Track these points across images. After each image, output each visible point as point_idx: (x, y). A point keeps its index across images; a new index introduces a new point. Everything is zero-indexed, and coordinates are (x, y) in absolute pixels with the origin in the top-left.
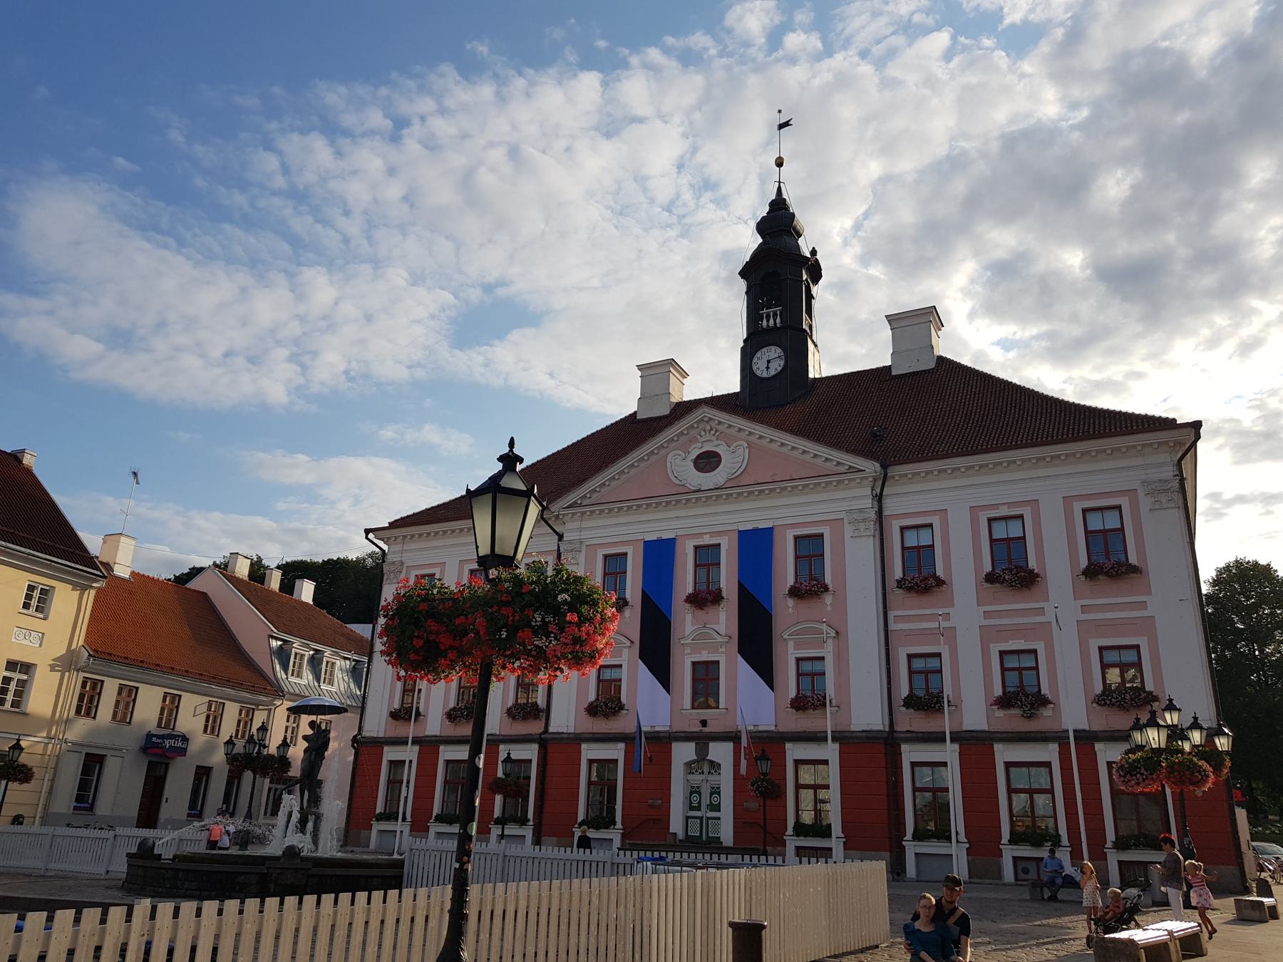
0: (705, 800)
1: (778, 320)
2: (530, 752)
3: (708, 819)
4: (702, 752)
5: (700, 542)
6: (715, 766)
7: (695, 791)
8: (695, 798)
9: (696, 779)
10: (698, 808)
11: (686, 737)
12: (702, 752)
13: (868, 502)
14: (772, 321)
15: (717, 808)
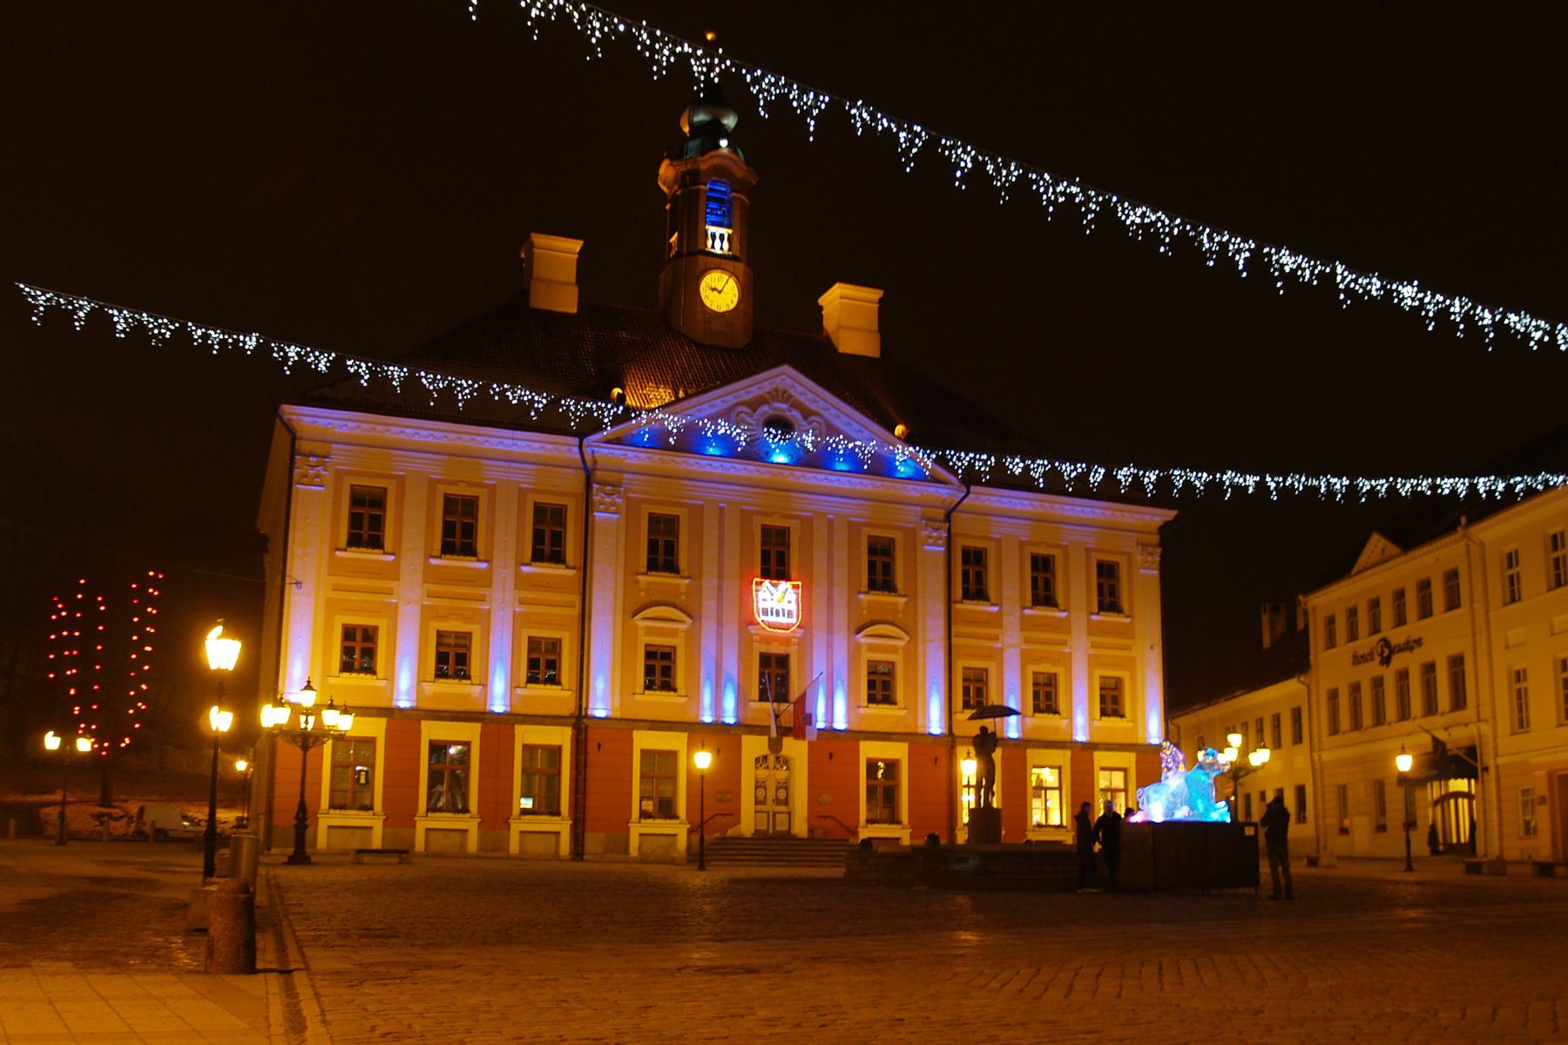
0: (771, 795)
1: (726, 245)
2: (561, 737)
3: (775, 814)
4: (775, 746)
5: (769, 522)
6: (786, 761)
7: (759, 785)
8: (761, 792)
9: (762, 773)
10: (763, 802)
11: (761, 730)
12: (775, 746)
13: (941, 514)
14: (718, 243)
15: (786, 802)
